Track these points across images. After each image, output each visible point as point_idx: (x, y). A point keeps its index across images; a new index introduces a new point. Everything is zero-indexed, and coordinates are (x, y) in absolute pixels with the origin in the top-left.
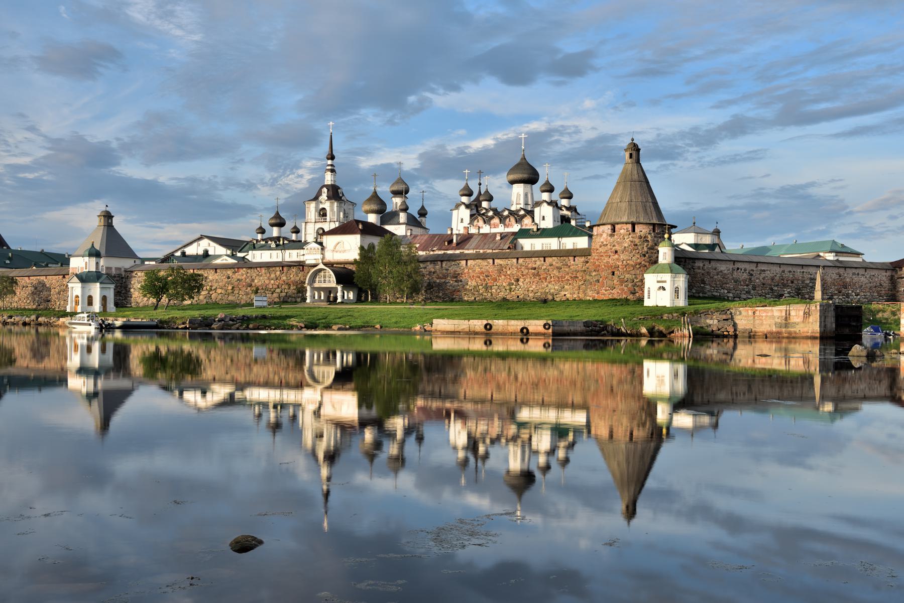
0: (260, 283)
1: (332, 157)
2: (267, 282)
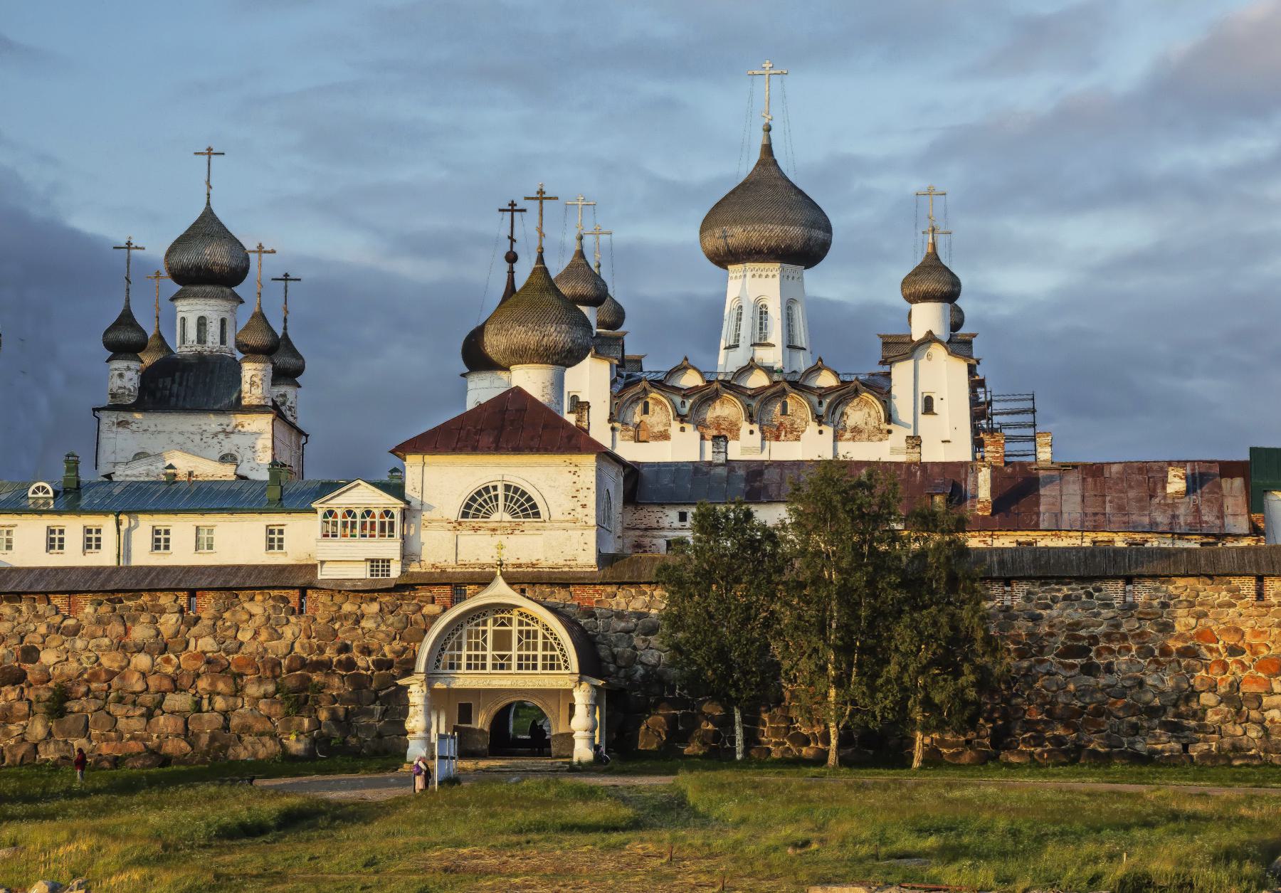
0: (72, 667)
2: (109, 661)
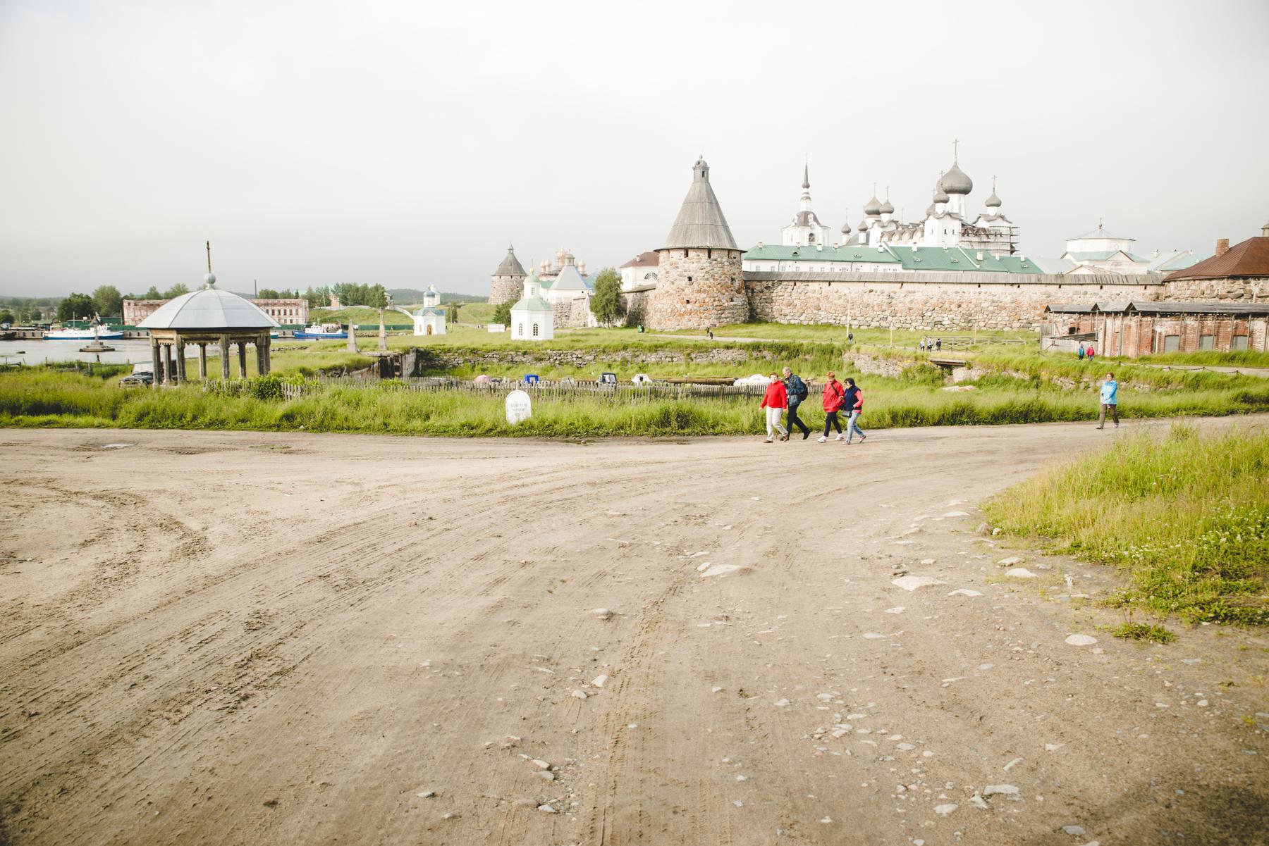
1: (807, 186)
